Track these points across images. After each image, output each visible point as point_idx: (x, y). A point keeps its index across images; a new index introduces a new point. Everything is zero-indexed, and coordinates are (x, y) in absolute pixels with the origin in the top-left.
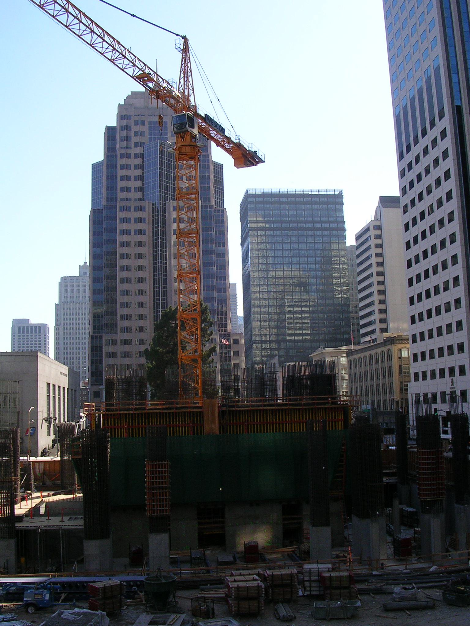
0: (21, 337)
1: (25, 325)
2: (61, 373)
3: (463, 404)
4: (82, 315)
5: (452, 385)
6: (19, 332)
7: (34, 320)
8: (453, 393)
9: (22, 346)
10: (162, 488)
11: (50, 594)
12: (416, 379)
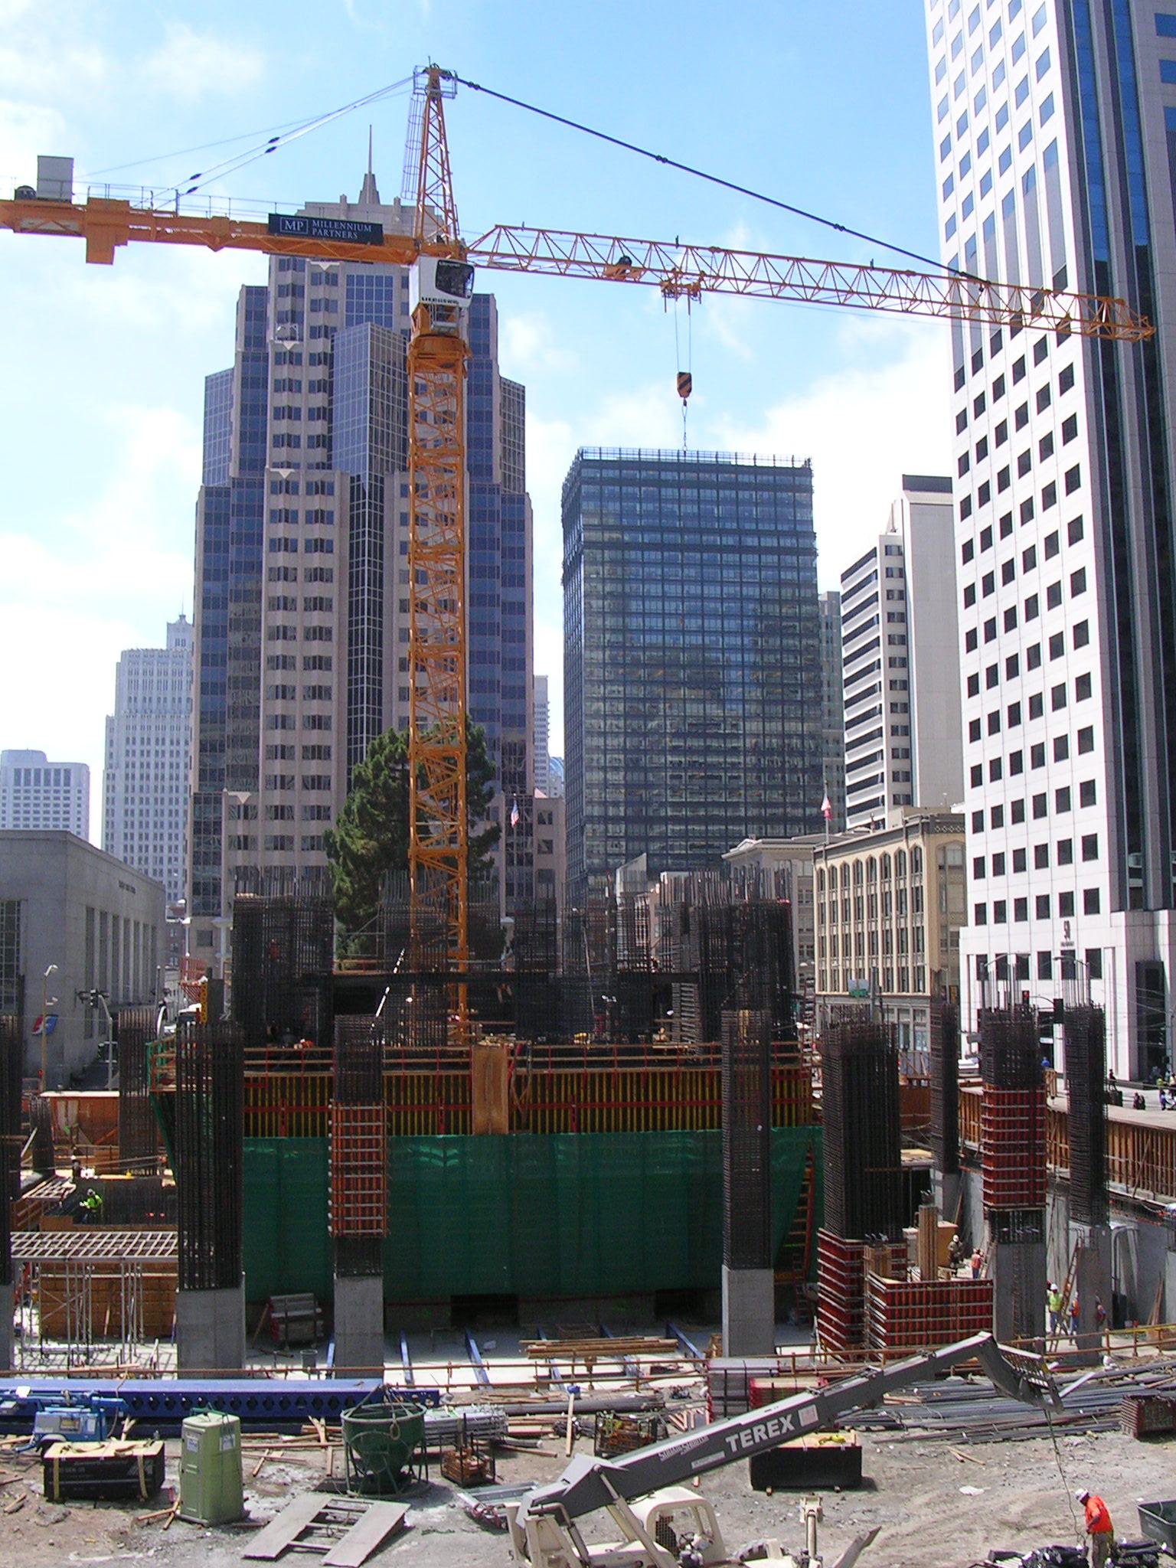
0: (22, 795)
1: (32, 766)
2: (122, 885)
3: (1094, 982)
4: (172, 743)
5: (1068, 935)
6: (17, 782)
7: (56, 755)
8: (1068, 956)
9: (22, 815)
10: (370, 1169)
11: (99, 1419)
12: (981, 919)
